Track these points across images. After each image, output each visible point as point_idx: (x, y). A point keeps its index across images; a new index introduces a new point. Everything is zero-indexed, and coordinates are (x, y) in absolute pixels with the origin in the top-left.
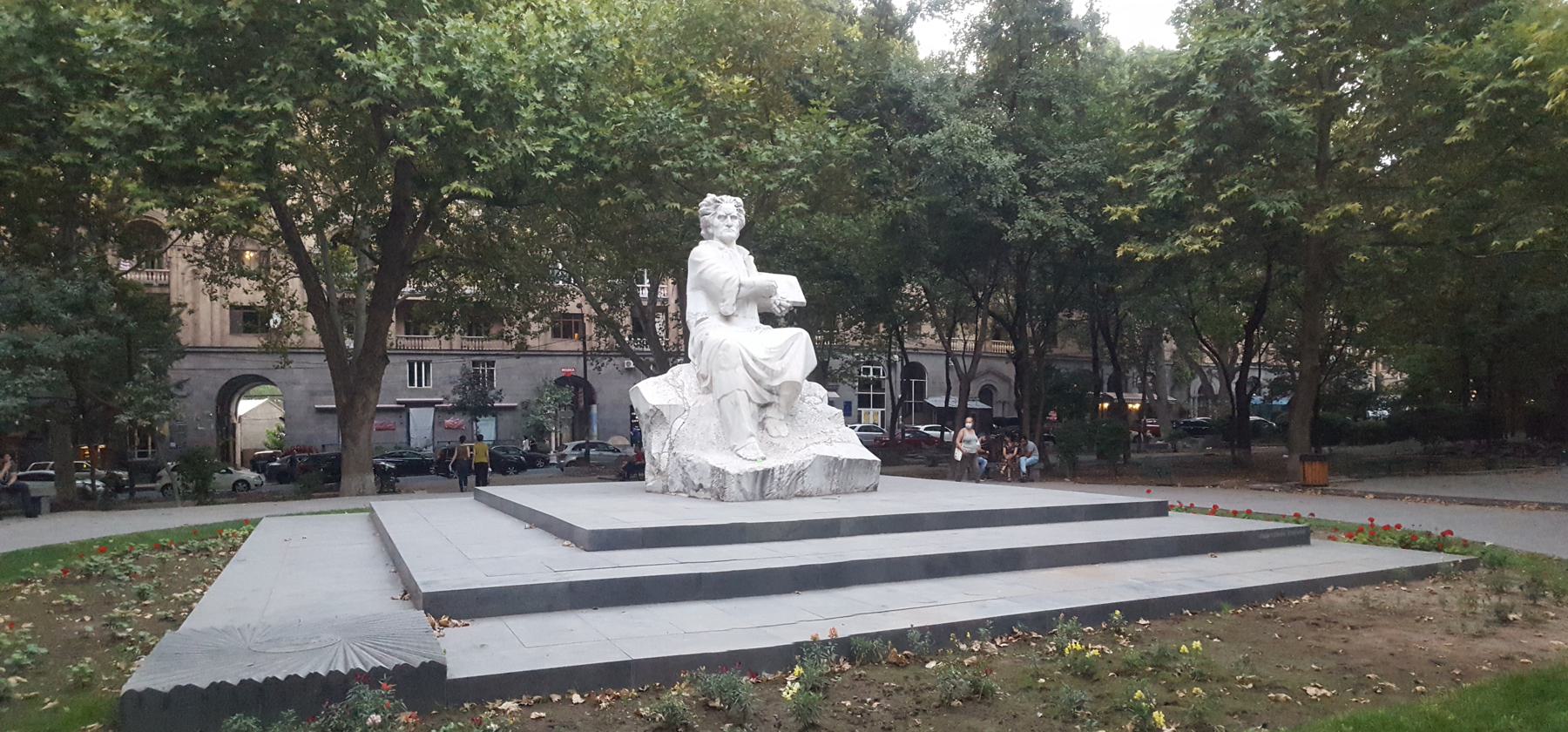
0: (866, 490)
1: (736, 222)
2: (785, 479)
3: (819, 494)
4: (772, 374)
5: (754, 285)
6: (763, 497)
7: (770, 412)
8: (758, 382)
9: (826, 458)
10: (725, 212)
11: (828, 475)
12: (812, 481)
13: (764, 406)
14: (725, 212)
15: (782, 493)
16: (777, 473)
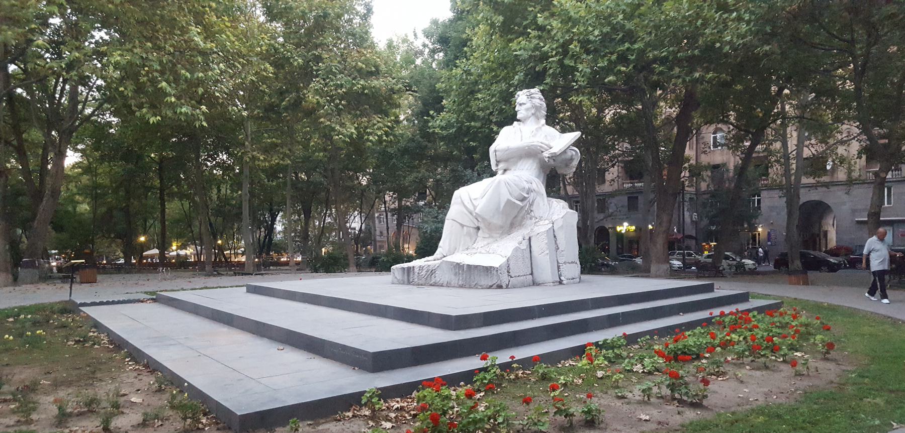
0: (490, 287)
1: (529, 105)
2: (424, 273)
3: (448, 285)
4: (475, 207)
5: (508, 149)
6: (409, 283)
7: (480, 231)
8: (471, 213)
9: (451, 263)
10: (529, 101)
11: (455, 274)
12: (440, 277)
13: (478, 228)
14: (529, 101)
15: (420, 282)
16: (416, 270)
